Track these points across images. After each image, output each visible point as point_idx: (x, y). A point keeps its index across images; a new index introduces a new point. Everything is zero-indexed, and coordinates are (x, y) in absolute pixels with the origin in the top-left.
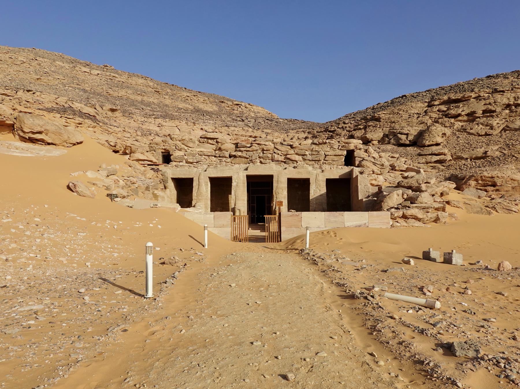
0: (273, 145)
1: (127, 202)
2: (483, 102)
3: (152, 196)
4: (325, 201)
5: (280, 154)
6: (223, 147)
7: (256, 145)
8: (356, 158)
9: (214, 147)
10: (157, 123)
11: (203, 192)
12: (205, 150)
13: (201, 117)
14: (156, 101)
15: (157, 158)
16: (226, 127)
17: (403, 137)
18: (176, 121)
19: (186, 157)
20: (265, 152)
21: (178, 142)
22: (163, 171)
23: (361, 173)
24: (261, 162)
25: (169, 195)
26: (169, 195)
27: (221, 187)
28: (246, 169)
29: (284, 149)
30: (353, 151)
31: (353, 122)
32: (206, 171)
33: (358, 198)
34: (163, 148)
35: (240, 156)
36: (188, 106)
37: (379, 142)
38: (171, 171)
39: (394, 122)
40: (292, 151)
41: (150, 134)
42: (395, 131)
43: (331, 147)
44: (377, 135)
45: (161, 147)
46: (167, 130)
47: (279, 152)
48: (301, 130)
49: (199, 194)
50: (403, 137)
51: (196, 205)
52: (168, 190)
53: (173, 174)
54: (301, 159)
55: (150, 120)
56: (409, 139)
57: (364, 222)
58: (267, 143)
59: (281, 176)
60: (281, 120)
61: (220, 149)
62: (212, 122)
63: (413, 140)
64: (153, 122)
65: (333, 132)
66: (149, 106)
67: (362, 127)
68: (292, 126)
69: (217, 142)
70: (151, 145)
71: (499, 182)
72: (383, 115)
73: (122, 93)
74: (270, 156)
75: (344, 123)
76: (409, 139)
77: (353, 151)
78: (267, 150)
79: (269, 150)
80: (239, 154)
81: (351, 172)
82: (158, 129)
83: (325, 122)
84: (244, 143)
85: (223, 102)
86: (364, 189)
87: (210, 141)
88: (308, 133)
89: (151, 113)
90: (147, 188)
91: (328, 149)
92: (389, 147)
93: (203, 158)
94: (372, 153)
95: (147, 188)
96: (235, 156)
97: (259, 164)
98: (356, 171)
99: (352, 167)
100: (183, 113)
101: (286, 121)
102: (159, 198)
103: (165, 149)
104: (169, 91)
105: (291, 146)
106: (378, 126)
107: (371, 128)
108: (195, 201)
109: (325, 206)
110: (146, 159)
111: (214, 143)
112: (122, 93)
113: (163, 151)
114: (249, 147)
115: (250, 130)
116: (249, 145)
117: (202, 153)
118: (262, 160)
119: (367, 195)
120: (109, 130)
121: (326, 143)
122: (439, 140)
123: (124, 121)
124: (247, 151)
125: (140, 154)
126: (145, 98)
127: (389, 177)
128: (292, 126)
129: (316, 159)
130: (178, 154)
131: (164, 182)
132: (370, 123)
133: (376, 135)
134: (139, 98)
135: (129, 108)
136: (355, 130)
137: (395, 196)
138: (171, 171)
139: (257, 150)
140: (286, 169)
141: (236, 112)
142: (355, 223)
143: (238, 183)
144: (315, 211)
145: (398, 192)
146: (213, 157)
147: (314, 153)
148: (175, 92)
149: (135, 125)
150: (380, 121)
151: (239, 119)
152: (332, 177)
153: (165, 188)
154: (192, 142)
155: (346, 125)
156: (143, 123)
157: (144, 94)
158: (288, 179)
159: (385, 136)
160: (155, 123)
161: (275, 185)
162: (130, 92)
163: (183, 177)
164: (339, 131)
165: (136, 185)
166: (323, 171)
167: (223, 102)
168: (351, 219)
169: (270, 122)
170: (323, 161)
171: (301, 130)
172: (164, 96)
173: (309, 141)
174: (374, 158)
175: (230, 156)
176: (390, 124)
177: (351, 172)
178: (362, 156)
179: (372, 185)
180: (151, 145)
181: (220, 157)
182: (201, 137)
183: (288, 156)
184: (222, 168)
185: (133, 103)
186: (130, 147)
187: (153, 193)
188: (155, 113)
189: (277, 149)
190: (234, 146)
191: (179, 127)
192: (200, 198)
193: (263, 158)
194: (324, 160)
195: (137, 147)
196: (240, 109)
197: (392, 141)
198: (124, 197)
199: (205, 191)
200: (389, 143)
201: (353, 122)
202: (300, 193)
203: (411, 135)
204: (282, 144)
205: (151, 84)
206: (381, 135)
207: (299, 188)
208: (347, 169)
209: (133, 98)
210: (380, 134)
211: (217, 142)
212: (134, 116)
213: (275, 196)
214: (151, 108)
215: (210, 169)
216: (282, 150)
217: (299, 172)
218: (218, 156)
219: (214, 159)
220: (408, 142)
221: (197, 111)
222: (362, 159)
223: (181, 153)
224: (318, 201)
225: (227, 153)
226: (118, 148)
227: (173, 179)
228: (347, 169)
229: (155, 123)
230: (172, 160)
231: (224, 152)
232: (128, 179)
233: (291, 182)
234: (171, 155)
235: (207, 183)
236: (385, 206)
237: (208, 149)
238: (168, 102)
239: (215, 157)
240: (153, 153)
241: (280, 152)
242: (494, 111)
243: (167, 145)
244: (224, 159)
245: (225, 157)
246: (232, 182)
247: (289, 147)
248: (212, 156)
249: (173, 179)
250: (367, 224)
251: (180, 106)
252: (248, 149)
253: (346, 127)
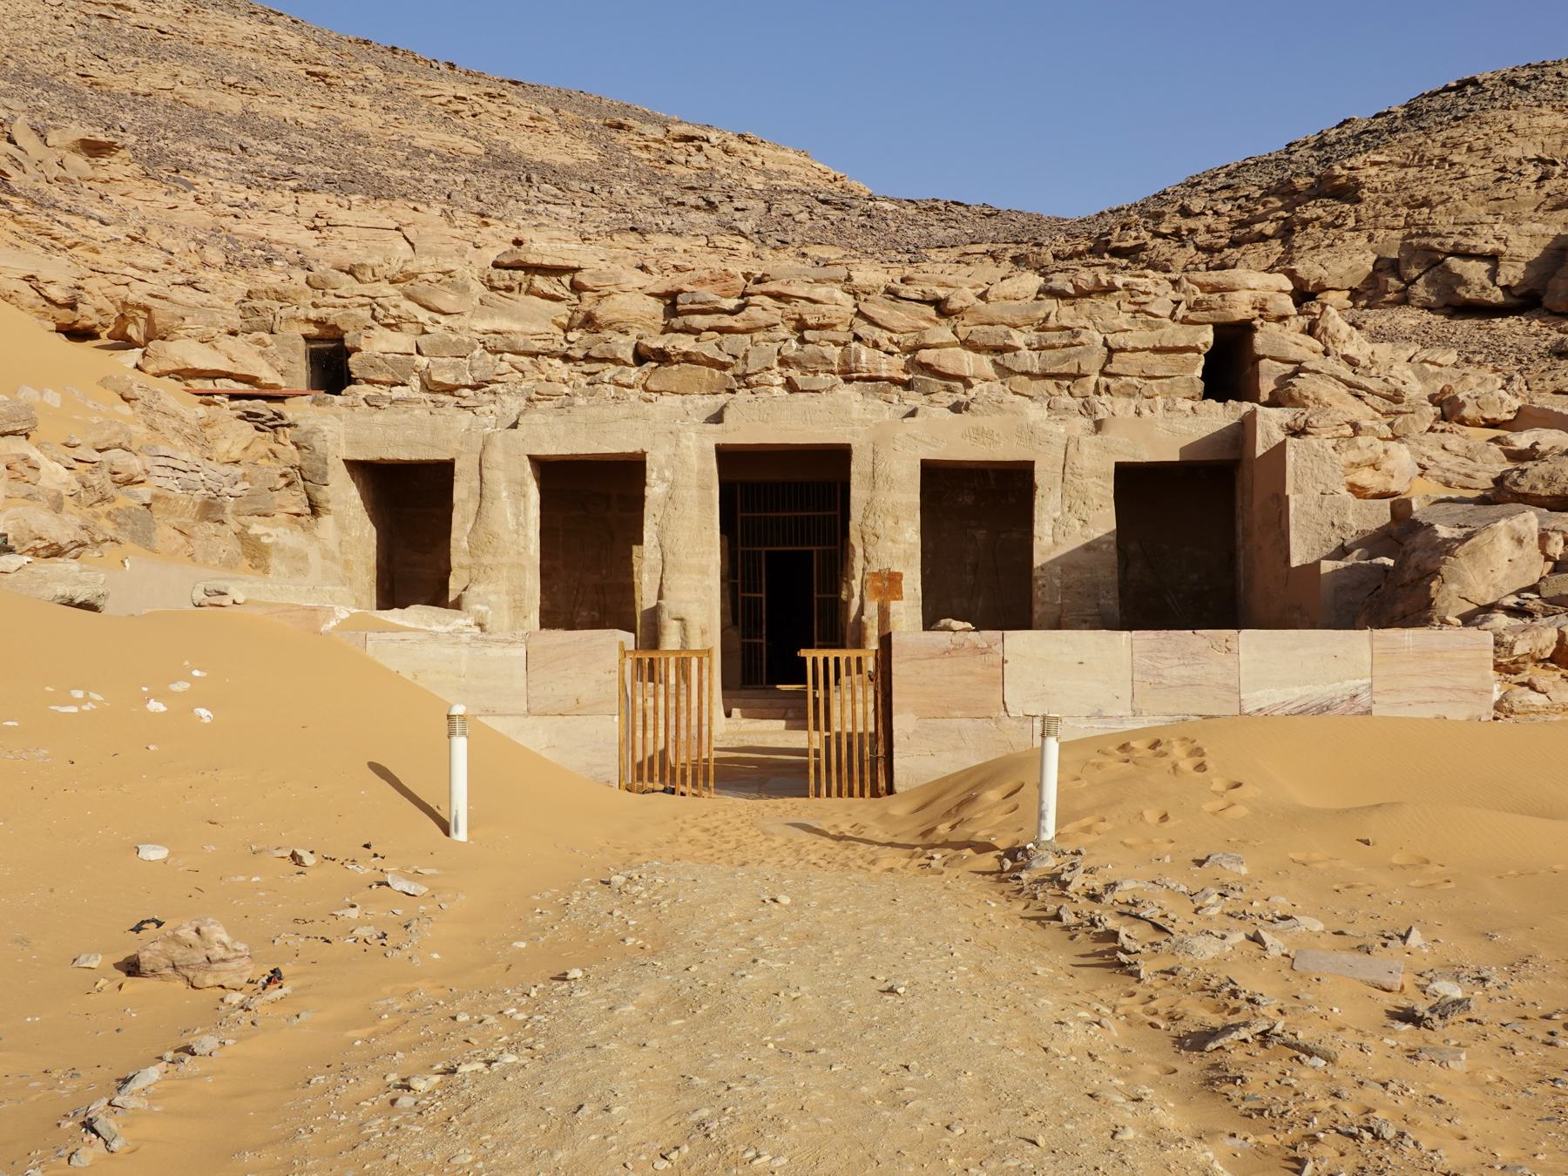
0: (848, 301)
1: (69, 577)
3: (234, 547)
4: (1108, 574)
5: (885, 343)
6: (603, 312)
7: (768, 302)
8: (1264, 363)
9: (561, 311)
10: (306, 212)
11: (500, 531)
12: (516, 327)
13: (517, 188)
14: (309, 117)
15: (282, 364)
16: (633, 236)
17: (1475, 271)
18: (399, 202)
19: (422, 361)
20: (808, 335)
21: (385, 288)
22: (304, 425)
23: (1297, 432)
24: (791, 386)
25: (332, 545)
26: (332, 545)
27: (591, 506)
28: (717, 418)
29: (903, 318)
30: (1245, 329)
31: (1225, 208)
32: (515, 426)
33: (1287, 559)
34: (313, 314)
35: (687, 357)
36: (457, 141)
37: (1355, 294)
38: (344, 429)
39: (1426, 202)
40: (942, 332)
41: (269, 261)
42: (1434, 243)
43: (1140, 309)
44: (1347, 263)
45: (301, 313)
46: (352, 246)
47: (877, 334)
48: (983, 248)
49: (482, 540)
50: (1475, 271)
51: (469, 597)
52: (326, 521)
53: (354, 443)
54: (989, 370)
55: (274, 198)
56: (1502, 281)
57: (1350, 685)
58: (819, 292)
59: (891, 452)
60: (887, 206)
61: (589, 322)
62: (565, 211)
63: (1523, 283)
64: (290, 209)
66: (277, 137)
67: (1269, 228)
68: (939, 233)
69: (576, 288)
70: (255, 303)
72: (1373, 171)
73: (154, 78)
74: (834, 353)
75: (1185, 212)
76: (1502, 281)
77: (1245, 329)
78: (820, 327)
79: (831, 326)
80: (686, 343)
82: (307, 239)
83: (1093, 213)
84: (708, 294)
85: (620, 126)
86: (1321, 510)
87: (539, 282)
89: (284, 167)
90: (210, 510)
91: (1123, 320)
92: (1408, 318)
93: (505, 366)
94: (1343, 335)
95: (210, 510)
96: (662, 357)
97: (778, 391)
98: (1270, 424)
99: (1246, 407)
100: (433, 169)
101: (911, 211)
102: (274, 562)
103: (319, 323)
104: (373, 72)
105: (941, 307)
106: (1351, 222)
107: (1315, 231)
108: (465, 575)
109: (1110, 602)
110: (224, 366)
111: (561, 291)
112: (154, 78)
113: (313, 330)
114: (732, 313)
115: (745, 247)
116: (731, 303)
117: (500, 343)
118: (794, 373)
119: (1336, 542)
120: (58, 230)
121: (1110, 289)
123: (147, 200)
124: (722, 330)
125: (194, 344)
126: (261, 105)
127: (1438, 454)
128: (939, 233)
129: (1064, 368)
130: (384, 346)
131: (306, 477)
132: (1312, 211)
133: (1345, 260)
134: (233, 103)
135: (181, 145)
136: (1235, 243)
137: (1505, 545)
138: (344, 429)
139: (769, 327)
140: (913, 414)
141: (682, 170)
142: (1297, 694)
143: (673, 486)
144: (1058, 625)
145: (1517, 522)
146: (557, 362)
147: (1053, 338)
148: (401, 81)
149: (203, 217)
150: (1359, 201)
151: (691, 199)
152: (1146, 455)
153: (315, 509)
154: (453, 286)
155: (1191, 223)
156: (238, 210)
157: (254, 84)
158: (923, 462)
159: (1386, 267)
160: (296, 214)
161: (858, 494)
162: (189, 73)
163: (405, 455)
165: (144, 492)
166: (1099, 426)
167: (620, 126)
168: (1274, 669)
169: (834, 215)
170: (1095, 377)
171: (983, 248)
172: (350, 96)
173: (1032, 281)
174: (1351, 362)
175: (640, 357)
176: (1405, 211)
177: (1243, 431)
178: (1294, 353)
179: (1357, 490)
180: (255, 303)
181: (588, 358)
182: (496, 265)
183: (925, 356)
184: (594, 411)
185: (200, 124)
186: (147, 309)
187: (242, 536)
188: (299, 169)
189: (872, 322)
190: (657, 307)
191: (410, 232)
192: (487, 560)
193: (799, 364)
194: (1103, 373)
195: (179, 311)
196: (698, 159)
197: (1420, 290)
198: (56, 552)
199: (512, 524)
200: (1404, 300)
201: (1225, 208)
202: (981, 534)
203: (1514, 258)
204: (893, 294)
205: (293, 42)
206: (1366, 262)
208: (1219, 416)
209: (204, 104)
210: (1358, 257)
211: (576, 288)
212: (200, 179)
213: (859, 551)
214: (286, 145)
215: (536, 417)
216: (894, 324)
217: (979, 433)
218: (579, 353)
219: (560, 368)
220: (1497, 296)
221: (502, 162)
222: (1289, 368)
223: (401, 342)
224: (1075, 575)
225: (622, 339)
226: (87, 315)
227: (354, 466)
228: (1219, 416)
229: (296, 214)
230: (356, 374)
231: (607, 333)
232: (97, 457)
233: (943, 483)
234: (349, 352)
235: (523, 484)
236: (1450, 597)
237: (533, 318)
238: (366, 120)
239: (566, 358)
240: (260, 342)
241: (882, 337)
243: (331, 299)
244: (610, 371)
245: (615, 361)
246: (644, 484)
247: (930, 311)
248: (551, 354)
249: (354, 466)
250: (1364, 699)
251: (421, 142)
252: (727, 321)
253: (1192, 231)
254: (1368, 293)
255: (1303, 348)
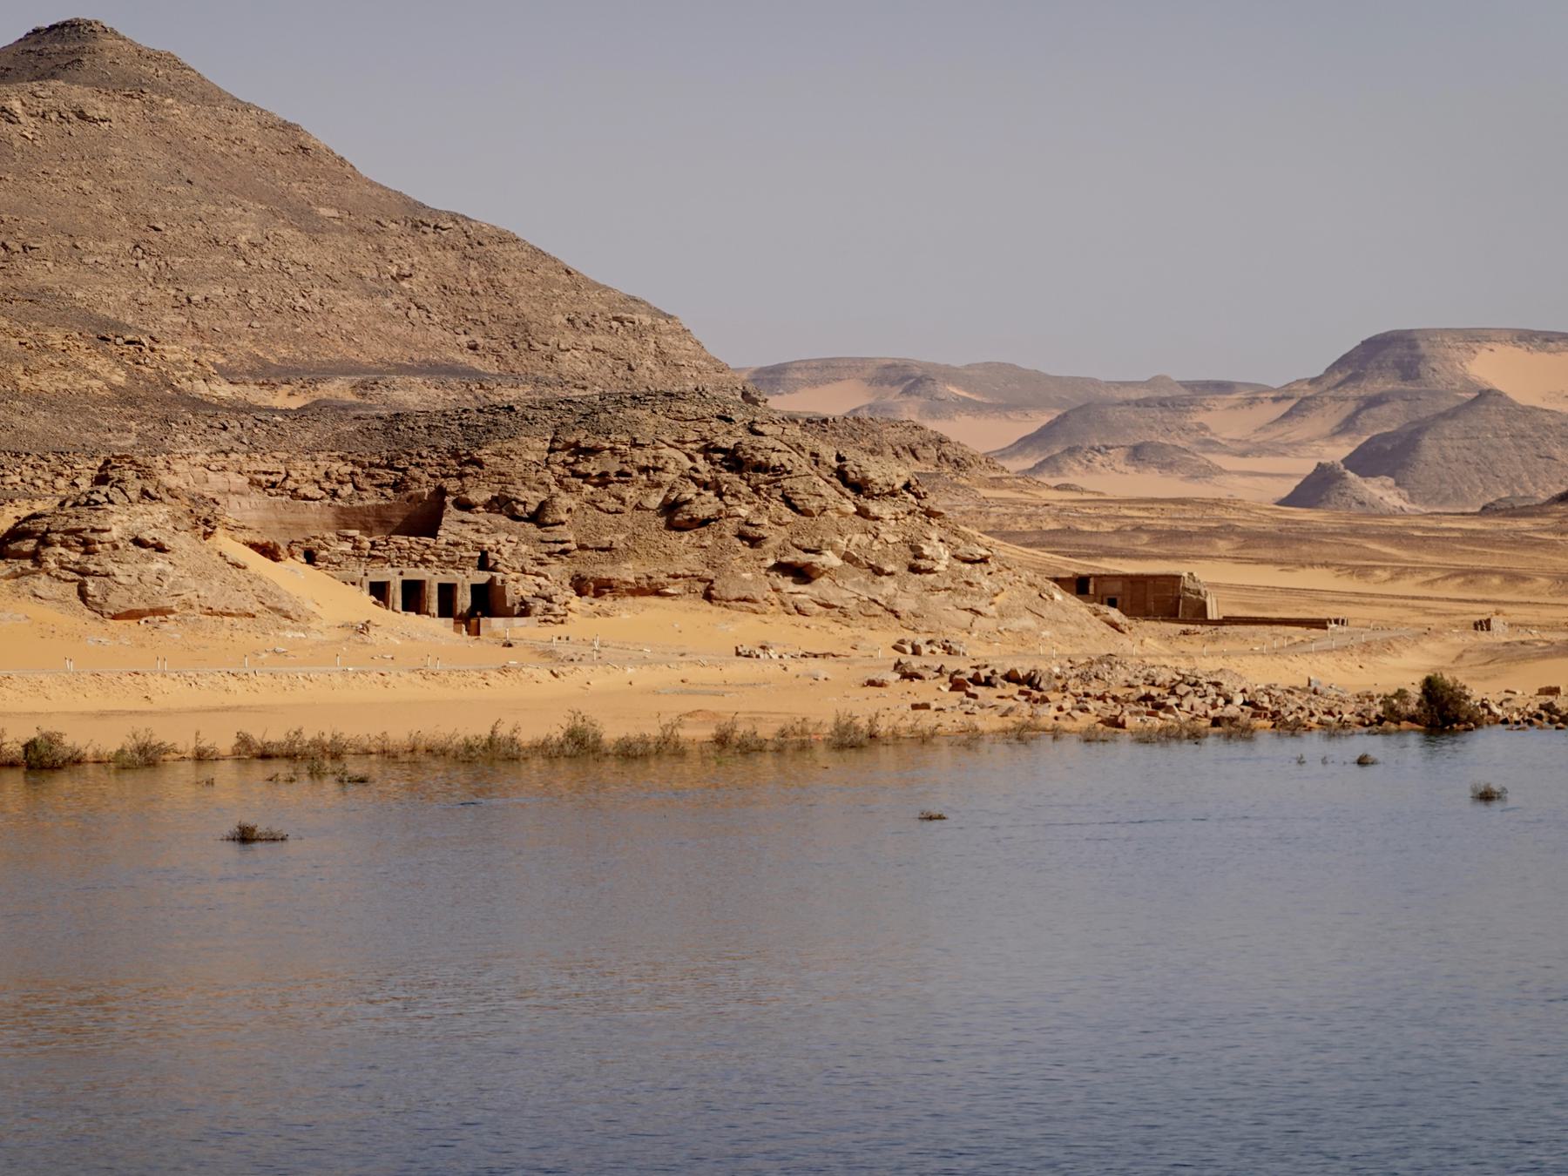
2: (618, 458)
17: (520, 507)
50: (520, 507)
61: (358, 548)
65: (404, 470)
71: (615, 583)
81: (493, 579)
85: (103, 339)
88: (353, 462)
96: (375, 557)
98: (499, 576)
105: (428, 547)
122: (564, 517)
132: (468, 470)
164: (416, 472)
177: (493, 579)
206: (489, 496)
207: (447, 592)
223: (324, 553)
242: (629, 475)
254: (490, 506)
255: (496, 556)
